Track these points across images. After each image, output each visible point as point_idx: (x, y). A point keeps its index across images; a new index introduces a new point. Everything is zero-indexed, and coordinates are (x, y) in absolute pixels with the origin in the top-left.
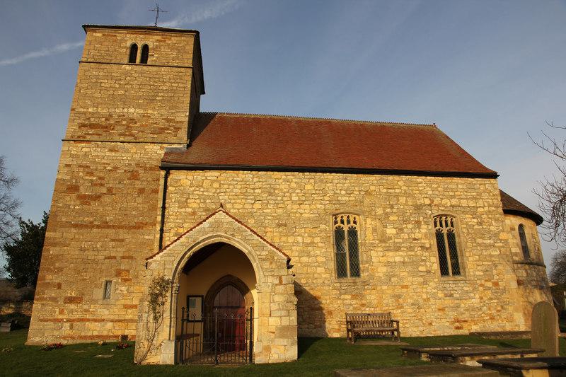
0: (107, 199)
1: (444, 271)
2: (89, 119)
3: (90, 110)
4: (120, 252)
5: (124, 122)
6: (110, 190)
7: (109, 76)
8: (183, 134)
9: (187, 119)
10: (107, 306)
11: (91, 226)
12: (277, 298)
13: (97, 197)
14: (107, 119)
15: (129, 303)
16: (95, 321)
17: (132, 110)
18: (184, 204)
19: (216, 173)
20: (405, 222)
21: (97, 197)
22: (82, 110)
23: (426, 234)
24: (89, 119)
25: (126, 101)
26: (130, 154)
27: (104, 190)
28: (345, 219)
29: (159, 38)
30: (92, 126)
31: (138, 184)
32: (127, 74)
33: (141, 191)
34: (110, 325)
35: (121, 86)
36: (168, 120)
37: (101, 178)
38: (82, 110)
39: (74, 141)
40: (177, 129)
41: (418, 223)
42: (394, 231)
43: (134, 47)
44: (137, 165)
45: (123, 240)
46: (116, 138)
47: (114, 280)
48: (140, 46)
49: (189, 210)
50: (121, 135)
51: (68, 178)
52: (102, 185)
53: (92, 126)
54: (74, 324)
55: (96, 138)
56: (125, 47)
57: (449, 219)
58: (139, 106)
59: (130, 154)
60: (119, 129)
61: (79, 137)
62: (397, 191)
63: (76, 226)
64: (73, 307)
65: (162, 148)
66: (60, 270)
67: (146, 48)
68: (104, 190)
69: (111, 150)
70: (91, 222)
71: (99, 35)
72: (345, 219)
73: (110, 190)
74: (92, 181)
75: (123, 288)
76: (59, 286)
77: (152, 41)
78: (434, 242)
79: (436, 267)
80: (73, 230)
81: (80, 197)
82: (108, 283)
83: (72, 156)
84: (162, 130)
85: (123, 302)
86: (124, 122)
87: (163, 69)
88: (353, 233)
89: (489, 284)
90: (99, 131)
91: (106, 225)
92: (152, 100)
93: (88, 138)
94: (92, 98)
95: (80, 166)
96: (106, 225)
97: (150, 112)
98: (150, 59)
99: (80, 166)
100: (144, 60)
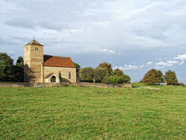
4: (38, 75)
7: (34, 52)
8: (43, 61)
23: (68, 74)
25: (36, 56)
26: (37, 64)
30: (33, 60)
53: (33, 60)
59: (37, 64)
67: (37, 48)
77: (38, 47)
88: (61, 74)
94: (32, 55)
100: (37, 50)
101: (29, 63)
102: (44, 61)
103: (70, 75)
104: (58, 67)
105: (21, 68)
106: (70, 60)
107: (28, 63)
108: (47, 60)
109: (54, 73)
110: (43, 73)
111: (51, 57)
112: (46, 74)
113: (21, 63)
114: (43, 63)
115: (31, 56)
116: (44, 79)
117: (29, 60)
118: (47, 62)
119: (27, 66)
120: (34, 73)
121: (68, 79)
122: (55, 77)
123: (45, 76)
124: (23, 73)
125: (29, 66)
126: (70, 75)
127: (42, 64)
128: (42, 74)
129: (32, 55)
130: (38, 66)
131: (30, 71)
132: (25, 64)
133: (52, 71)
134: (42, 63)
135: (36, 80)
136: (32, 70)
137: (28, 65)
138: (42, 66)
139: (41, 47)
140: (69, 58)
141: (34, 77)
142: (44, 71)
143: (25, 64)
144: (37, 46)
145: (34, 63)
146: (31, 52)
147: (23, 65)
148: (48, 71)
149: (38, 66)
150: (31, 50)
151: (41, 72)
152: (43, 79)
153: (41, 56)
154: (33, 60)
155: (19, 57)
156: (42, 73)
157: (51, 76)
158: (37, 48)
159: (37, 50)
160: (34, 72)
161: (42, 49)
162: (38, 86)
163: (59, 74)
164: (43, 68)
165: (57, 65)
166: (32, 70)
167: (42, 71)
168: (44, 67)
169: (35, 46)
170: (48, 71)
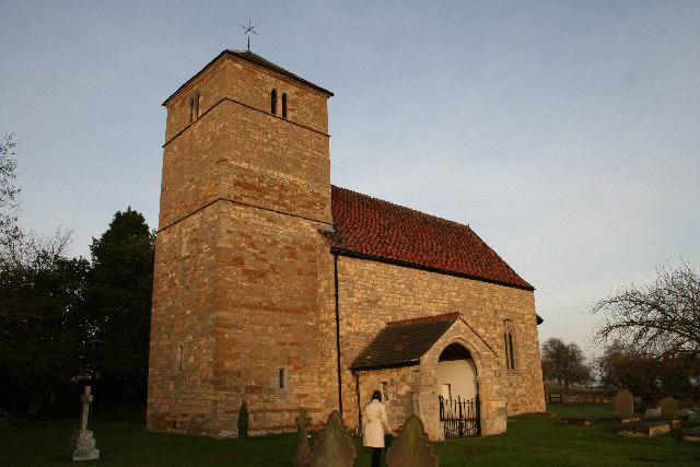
0: (270, 277)
2: (242, 176)
3: (244, 165)
8: (328, 210)
10: (283, 396)
11: (259, 306)
13: (263, 275)
14: (260, 181)
16: (276, 411)
18: (351, 295)
21: (263, 275)
24: (242, 176)
25: (275, 161)
26: (286, 230)
27: (267, 266)
29: (297, 89)
30: (247, 187)
32: (273, 126)
34: (287, 414)
35: (269, 144)
36: (317, 195)
39: (233, 202)
40: (323, 206)
43: (274, 93)
44: (294, 242)
46: (271, 206)
47: (287, 368)
48: (279, 95)
49: (355, 300)
50: (275, 203)
53: (247, 187)
54: (258, 415)
55: (252, 202)
58: (287, 171)
59: (286, 230)
63: (246, 306)
64: (255, 397)
65: (313, 226)
66: (236, 356)
67: (284, 96)
69: (270, 220)
70: (260, 303)
71: (239, 66)
74: (255, 255)
77: (291, 91)
80: (245, 311)
81: (246, 272)
82: (282, 371)
84: (311, 205)
91: (272, 308)
92: (297, 165)
93: (245, 200)
95: (242, 234)
96: (272, 308)
98: (290, 115)
99: (242, 234)
100: (284, 114)
104: (443, 272)
109: (454, 316)
112: (363, 327)
123: (355, 348)
130: (293, 255)
134: (325, 234)
139: (311, 96)
144: (284, 89)
149: (293, 255)
151: (316, 308)
158: (284, 96)
159: (284, 114)
161: (322, 116)
168: (344, 262)
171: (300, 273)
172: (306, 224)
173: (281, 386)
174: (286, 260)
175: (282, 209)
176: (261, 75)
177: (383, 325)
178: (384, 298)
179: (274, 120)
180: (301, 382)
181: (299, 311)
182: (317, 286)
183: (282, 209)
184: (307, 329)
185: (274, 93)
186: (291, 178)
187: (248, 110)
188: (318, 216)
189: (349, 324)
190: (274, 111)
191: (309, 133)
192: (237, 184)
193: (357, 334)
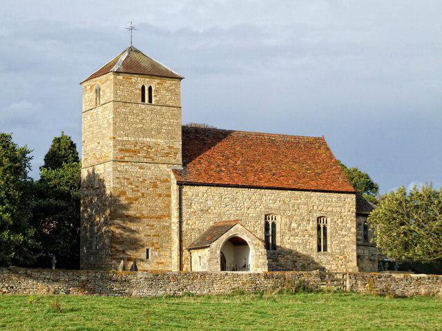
1: (319, 249)
3: (125, 138)
5: (145, 148)
6: (143, 194)
7: (131, 112)
8: (179, 156)
9: (180, 147)
10: (149, 263)
12: (261, 261)
13: (137, 199)
14: (135, 146)
15: (159, 261)
17: (148, 139)
18: (190, 206)
19: (206, 188)
20: (303, 220)
21: (137, 199)
22: (119, 138)
23: (313, 224)
25: (145, 132)
26: (151, 172)
27: (140, 194)
28: (270, 217)
30: (128, 151)
31: (158, 191)
32: (143, 111)
33: (160, 195)
37: (137, 187)
38: (119, 138)
40: (176, 153)
41: (309, 220)
42: (296, 225)
43: (143, 88)
45: (153, 226)
46: (142, 159)
48: (147, 88)
51: (119, 186)
52: (138, 191)
53: (128, 151)
56: (138, 89)
57: (325, 219)
59: (151, 172)
60: (142, 154)
61: (121, 158)
62: (299, 201)
67: (150, 89)
68: (140, 194)
69: (141, 168)
72: (270, 217)
73: (143, 194)
75: (156, 253)
76: (124, 252)
77: (154, 83)
78: (315, 232)
79: (315, 247)
83: (119, 171)
85: (156, 260)
86: (145, 148)
87: (164, 108)
88: (274, 225)
89: (341, 257)
90: (132, 154)
93: (126, 159)
97: (159, 140)
98: (153, 100)
100: (150, 101)
101: (106, 172)
102: (184, 157)
103: (321, 231)
104: (261, 188)
105: (65, 196)
106: (322, 151)
107: (100, 170)
108: (201, 151)
109: (236, 221)
110: (181, 222)
111: (220, 136)
112: (197, 225)
113: (66, 171)
114: (180, 168)
115: (115, 131)
116: (186, 253)
117: (110, 153)
118: (200, 164)
119: (95, 184)
120: (133, 226)
121: (315, 255)
122: (244, 243)
124: (78, 224)
125: (110, 187)
126: (321, 231)
127: (173, 176)
128: (175, 227)
129: (124, 130)
130: (155, 186)
131: (114, 215)
132: (84, 174)
133: (229, 214)
134: (175, 171)
135: (144, 256)
136: (125, 207)
137: (101, 181)
138: (175, 187)
139: (168, 83)
140: (320, 143)
141: (135, 244)
142: (184, 209)
143: (84, 174)
145: (134, 170)
146: (116, 113)
147: (76, 183)
148: (205, 211)
149: (155, 186)
150: (120, 102)
151: (169, 216)
152: (181, 256)
153: (168, 133)
154: (126, 153)
155: (58, 140)
156: (175, 219)
157: (224, 237)
158: (150, 89)
159: (150, 101)
160: (133, 219)
162: (152, 293)
163: (267, 224)
164: (180, 195)
165: (252, 178)
166: (125, 207)
167: (175, 213)
168: (186, 189)
169: (140, 81)
170: (205, 211)
171: (160, 195)
172: (165, 166)
173: (148, 257)
174: (151, 189)
175: (149, 160)
176: (134, 79)
177: (211, 224)
178: (212, 208)
179: (143, 106)
180: (160, 256)
181: (159, 218)
182: (170, 202)
183: (149, 160)
184: (164, 227)
185: (143, 88)
186: (154, 140)
187: (128, 105)
188: (173, 161)
189: (188, 224)
190: (143, 100)
191: (167, 108)
192: (121, 150)
193: (193, 230)
